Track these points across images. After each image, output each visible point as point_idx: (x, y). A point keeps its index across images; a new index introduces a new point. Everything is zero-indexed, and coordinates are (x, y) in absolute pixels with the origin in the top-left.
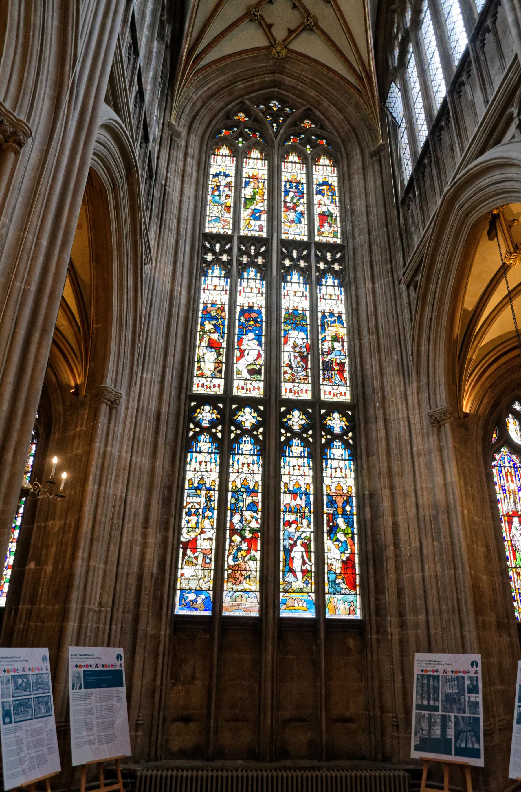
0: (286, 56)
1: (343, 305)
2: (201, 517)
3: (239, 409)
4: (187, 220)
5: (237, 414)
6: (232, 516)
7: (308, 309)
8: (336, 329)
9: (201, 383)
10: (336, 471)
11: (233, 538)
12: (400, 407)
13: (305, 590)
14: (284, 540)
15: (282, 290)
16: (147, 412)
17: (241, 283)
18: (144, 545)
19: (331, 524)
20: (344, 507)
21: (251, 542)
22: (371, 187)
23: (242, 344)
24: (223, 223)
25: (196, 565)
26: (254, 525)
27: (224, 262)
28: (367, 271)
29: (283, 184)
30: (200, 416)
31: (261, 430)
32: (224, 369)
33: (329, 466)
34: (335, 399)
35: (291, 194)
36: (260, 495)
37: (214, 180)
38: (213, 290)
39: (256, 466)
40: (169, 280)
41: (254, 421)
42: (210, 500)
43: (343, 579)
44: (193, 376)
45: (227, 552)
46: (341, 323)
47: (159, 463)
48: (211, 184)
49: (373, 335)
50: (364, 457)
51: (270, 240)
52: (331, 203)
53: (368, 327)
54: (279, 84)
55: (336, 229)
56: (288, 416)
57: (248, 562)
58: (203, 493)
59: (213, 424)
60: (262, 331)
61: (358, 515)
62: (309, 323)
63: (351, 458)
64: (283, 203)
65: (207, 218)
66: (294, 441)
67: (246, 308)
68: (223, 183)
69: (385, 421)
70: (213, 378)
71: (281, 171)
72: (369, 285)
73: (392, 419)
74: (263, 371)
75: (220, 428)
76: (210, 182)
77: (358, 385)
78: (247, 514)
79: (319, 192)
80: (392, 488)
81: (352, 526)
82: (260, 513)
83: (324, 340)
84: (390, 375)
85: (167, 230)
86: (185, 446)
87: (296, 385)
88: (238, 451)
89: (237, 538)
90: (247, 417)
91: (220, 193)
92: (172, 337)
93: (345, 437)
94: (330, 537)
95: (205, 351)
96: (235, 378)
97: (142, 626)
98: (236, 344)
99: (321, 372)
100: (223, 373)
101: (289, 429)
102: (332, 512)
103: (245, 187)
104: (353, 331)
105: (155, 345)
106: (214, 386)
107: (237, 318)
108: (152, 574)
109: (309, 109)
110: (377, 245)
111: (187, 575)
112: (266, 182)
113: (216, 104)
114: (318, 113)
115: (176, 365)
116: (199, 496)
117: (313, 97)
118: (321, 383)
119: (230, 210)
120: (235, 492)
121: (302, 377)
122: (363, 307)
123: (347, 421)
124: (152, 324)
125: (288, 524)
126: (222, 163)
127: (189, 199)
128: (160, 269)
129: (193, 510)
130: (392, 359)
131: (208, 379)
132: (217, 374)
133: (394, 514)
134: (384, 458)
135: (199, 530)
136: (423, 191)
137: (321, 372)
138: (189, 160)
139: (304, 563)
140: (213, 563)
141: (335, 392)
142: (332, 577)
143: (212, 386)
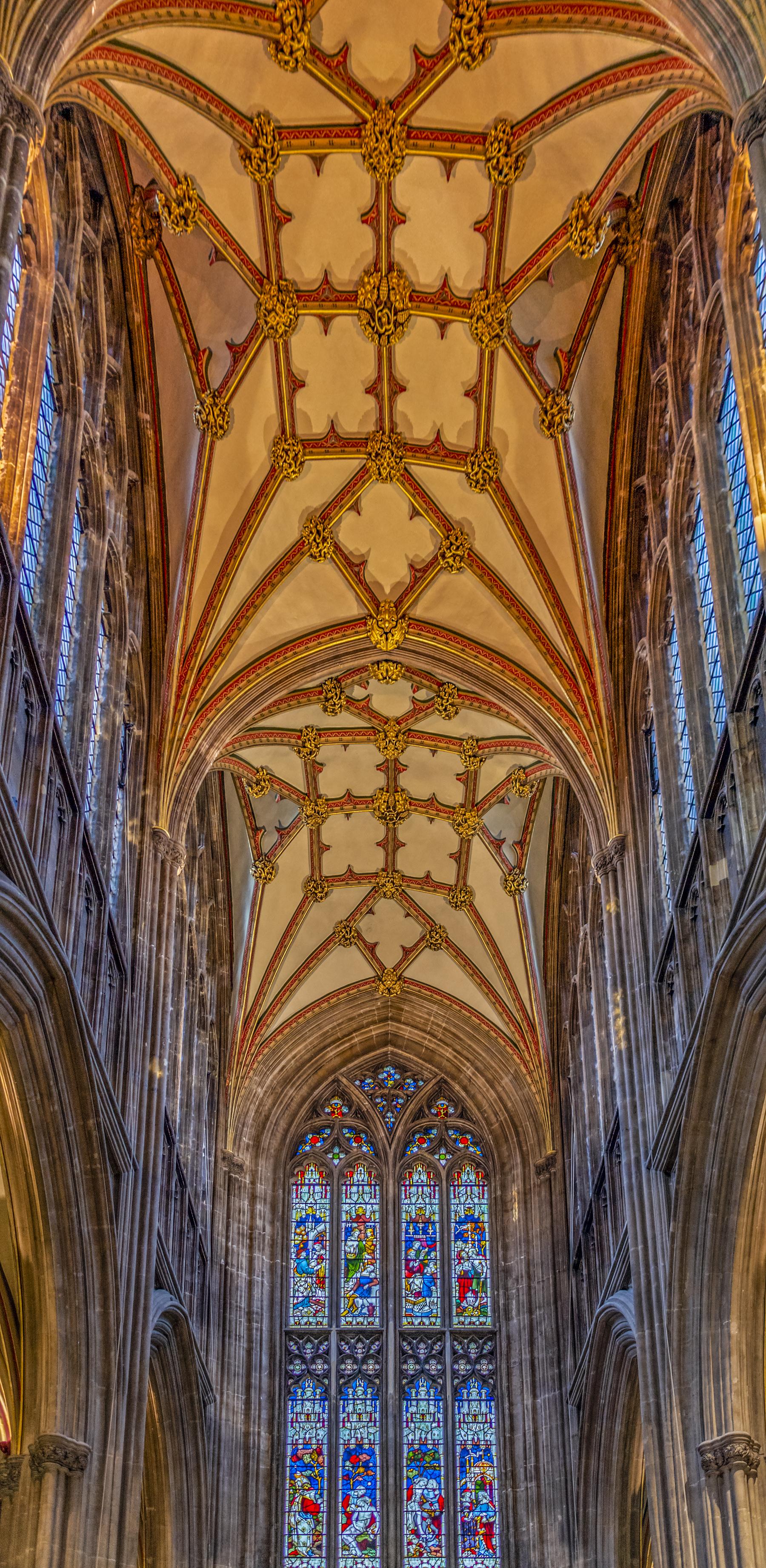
17: (344, 1407)
23: (348, 1505)
29: (404, 1225)
35: (417, 1245)
37: (298, 1231)
40: (241, 1418)
44: (282, 1557)
46: (490, 1459)
48: (295, 1240)
52: (478, 1254)
53: (526, 1468)
67: (352, 1447)
68: (312, 1235)
72: (528, 1401)
79: (460, 1236)
87: (425, 1560)
91: (308, 1255)
99: (460, 1539)
103: (346, 1240)
104: (506, 1474)
112: (378, 1225)
114: (457, 1088)
117: (448, 1060)
119: (324, 1283)
121: (433, 1548)
122: (519, 1435)
137: (460, 1539)
138: (259, 1207)
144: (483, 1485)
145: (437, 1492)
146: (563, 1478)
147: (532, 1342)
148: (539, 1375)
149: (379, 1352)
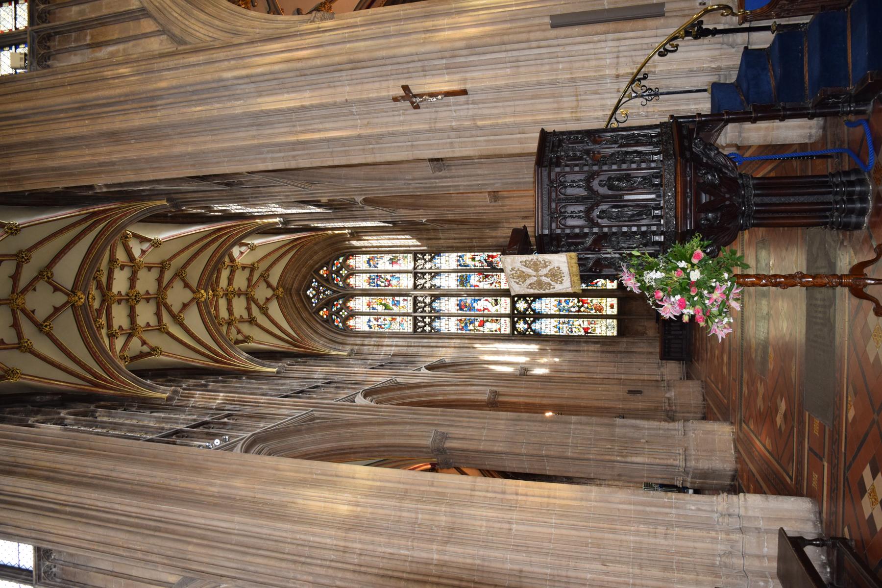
3: (517, 310)
18: (588, 351)
21: (583, 302)
26: (576, 301)
35: (379, 283)
38: (448, 325)
48: (377, 329)
54: (298, 291)
59: (526, 322)
68: (375, 323)
72: (442, 241)
78: (571, 304)
89: (582, 309)
97: (623, 350)
113: (321, 329)
120: (560, 310)
126: (360, 324)
135: (578, 327)
138: (366, 343)
144: (473, 259)
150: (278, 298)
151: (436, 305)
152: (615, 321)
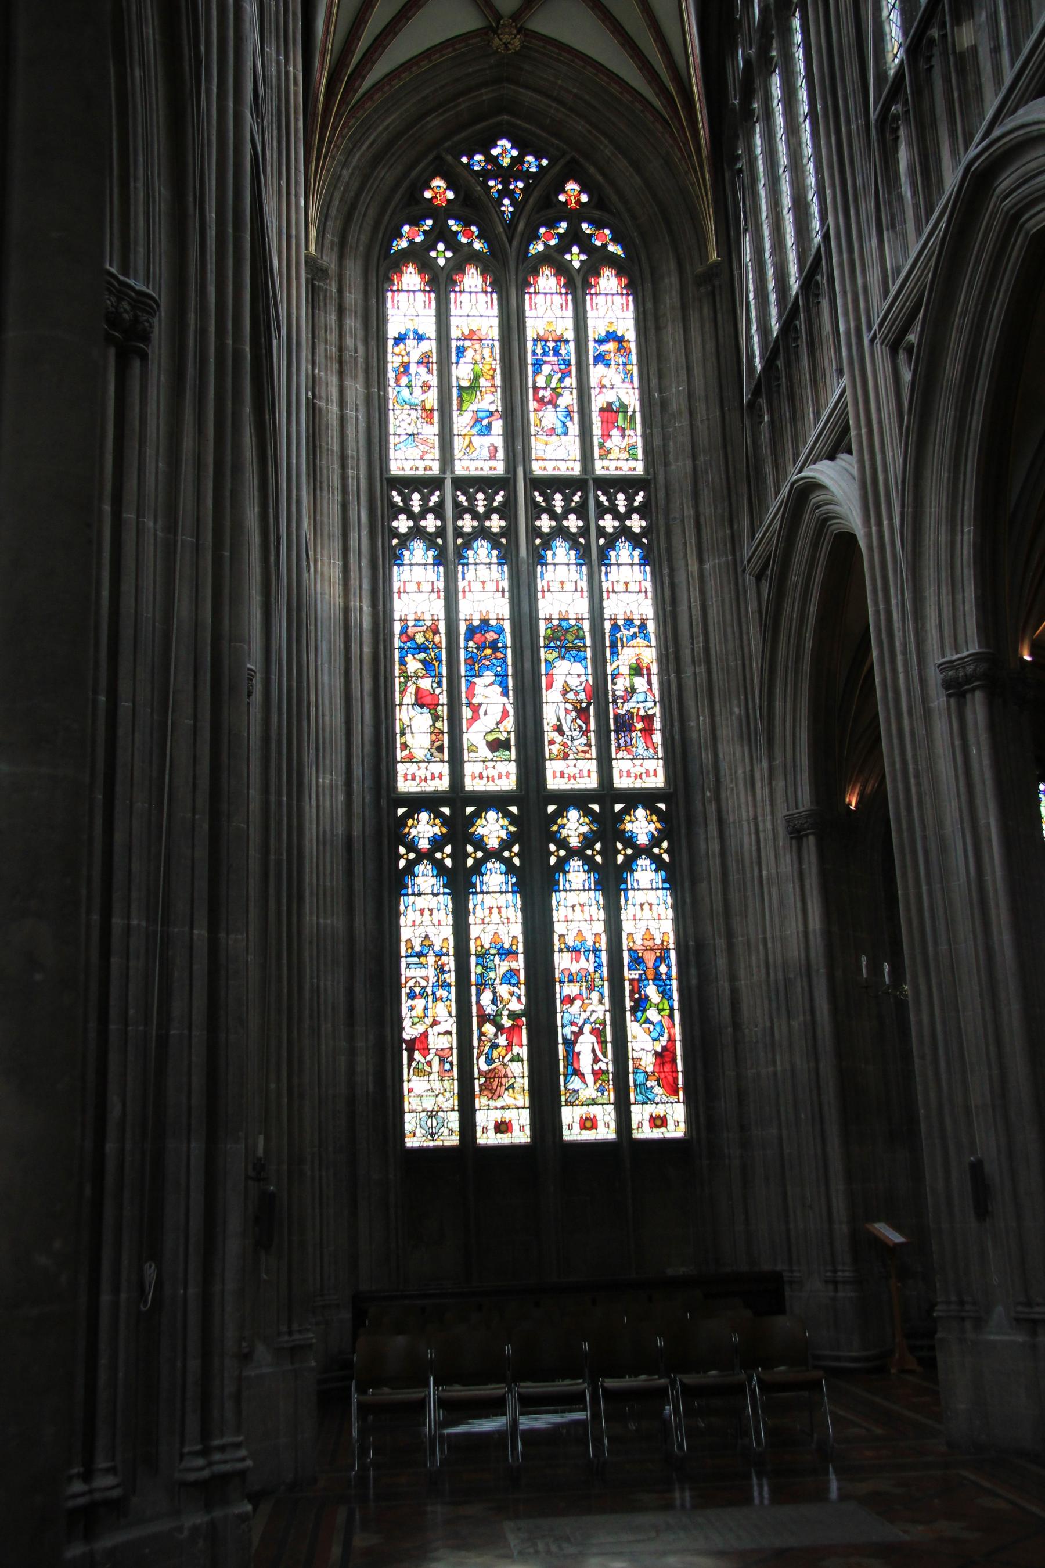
0: (523, 47)
1: (649, 602)
2: (430, 999)
3: (477, 815)
4: (358, 460)
5: (474, 824)
6: (479, 995)
7: (586, 616)
8: (637, 651)
9: (410, 773)
10: (642, 909)
11: (483, 1030)
12: (743, 800)
13: (600, 1101)
14: (563, 1026)
15: (539, 580)
16: (332, 842)
17: (463, 574)
19: (637, 996)
20: (656, 968)
22: (697, 354)
23: (474, 695)
24: (422, 447)
25: (430, 1074)
26: (516, 1006)
27: (430, 534)
28: (690, 538)
29: (530, 345)
30: (414, 832)
31: (516, 848)
32: (446, 745)
33: (630, 902)
34: (638, 784)
35: (546, 369)
36: (521, 957)
37: (397, 350)
38: (415, 591)
39: (511, 909)
40: (338, 590)
41: (503, 834)
42: (443, 972)
43: (658, 1080)
44: (395, 762)
45: (475, 1051)
46: (646, 637)
47: (359, 922)
48: (393, 361)
49: (700, 665)
50: (687, 884)
51: (512, 482)
53: (693, 649)
55: (634, 439)
56: (559, 821)
57: (510, 1064)
58: (431, 960)
59: (437, 843)
60: (507, 666)
61: (680, 979)
62: (588, 642)
63: (667, 886)
64: (531, 391)
65: (391, 438)
66: (572, 863)
67: (476, 623)
68: (415, 356)
69: (721, 821)
70: (429, 762)
71: (524, 317)
72: (694, 567)
73: (731, 820)
74: (513, 742)
75: (448, 849)
76: (390, 357)
77: (677, 756)
78: (503, 990)
79: (600, 358)
80: (730, 935)
81: (670, 998)
82: (523, 987)
83: (615, 676)
84: (728, 742)
85: (325, 493)
86: (394, 884)
88: (481, 887)
89: (489, 1029)
90: (492, 828)
92: (356, 700)
93: (656, 850)
94: (636, 1017)
95: (412, 713)
96: (466, 758)
98: (463, 695)
99: (613, 735)
100: (446, 751)
101: (563, 844)
102: (637, 977)
103: (457, 363)
105: (331, 720)
106: (433, 778)
107: (462, 645)
108: (368, 1093)
109: (573, 160)
110: (708, 486)
111: (416, 1091)
112: (497, 344)
113: (386, 175)
114: (592, 170)
115: (368, 748)
116: (423, 966)
118: (614, 756)
119: (432, 418)
120: (482, 955)
121: (581, 748)
122: (683, 607)
123: (658, 821)
124: (323, 684)
125: (570, 1000)
126: (408, 307)
127: (357, 410)
128: (322, 573)
129: (417, 990)
130: (731, 713)
131: (420, 764)
132: (436, 754)
133: (733, 978)
134: (717, 887)
135: (427, 1018)
136: (776, 416)
138: (349, 322)
139: (596, 1060)
140: (455, 1069)
141: (638, 770)
142: (641, 1078)
143: (429, 778)
144: (637, 670)
145: (583, 678)
146: (739, 662)
147: (696, 495)
148: (706, 532)
149: (504, 504)
150: (489, 30)
151: (482, 550)
152: (454, 1140)
